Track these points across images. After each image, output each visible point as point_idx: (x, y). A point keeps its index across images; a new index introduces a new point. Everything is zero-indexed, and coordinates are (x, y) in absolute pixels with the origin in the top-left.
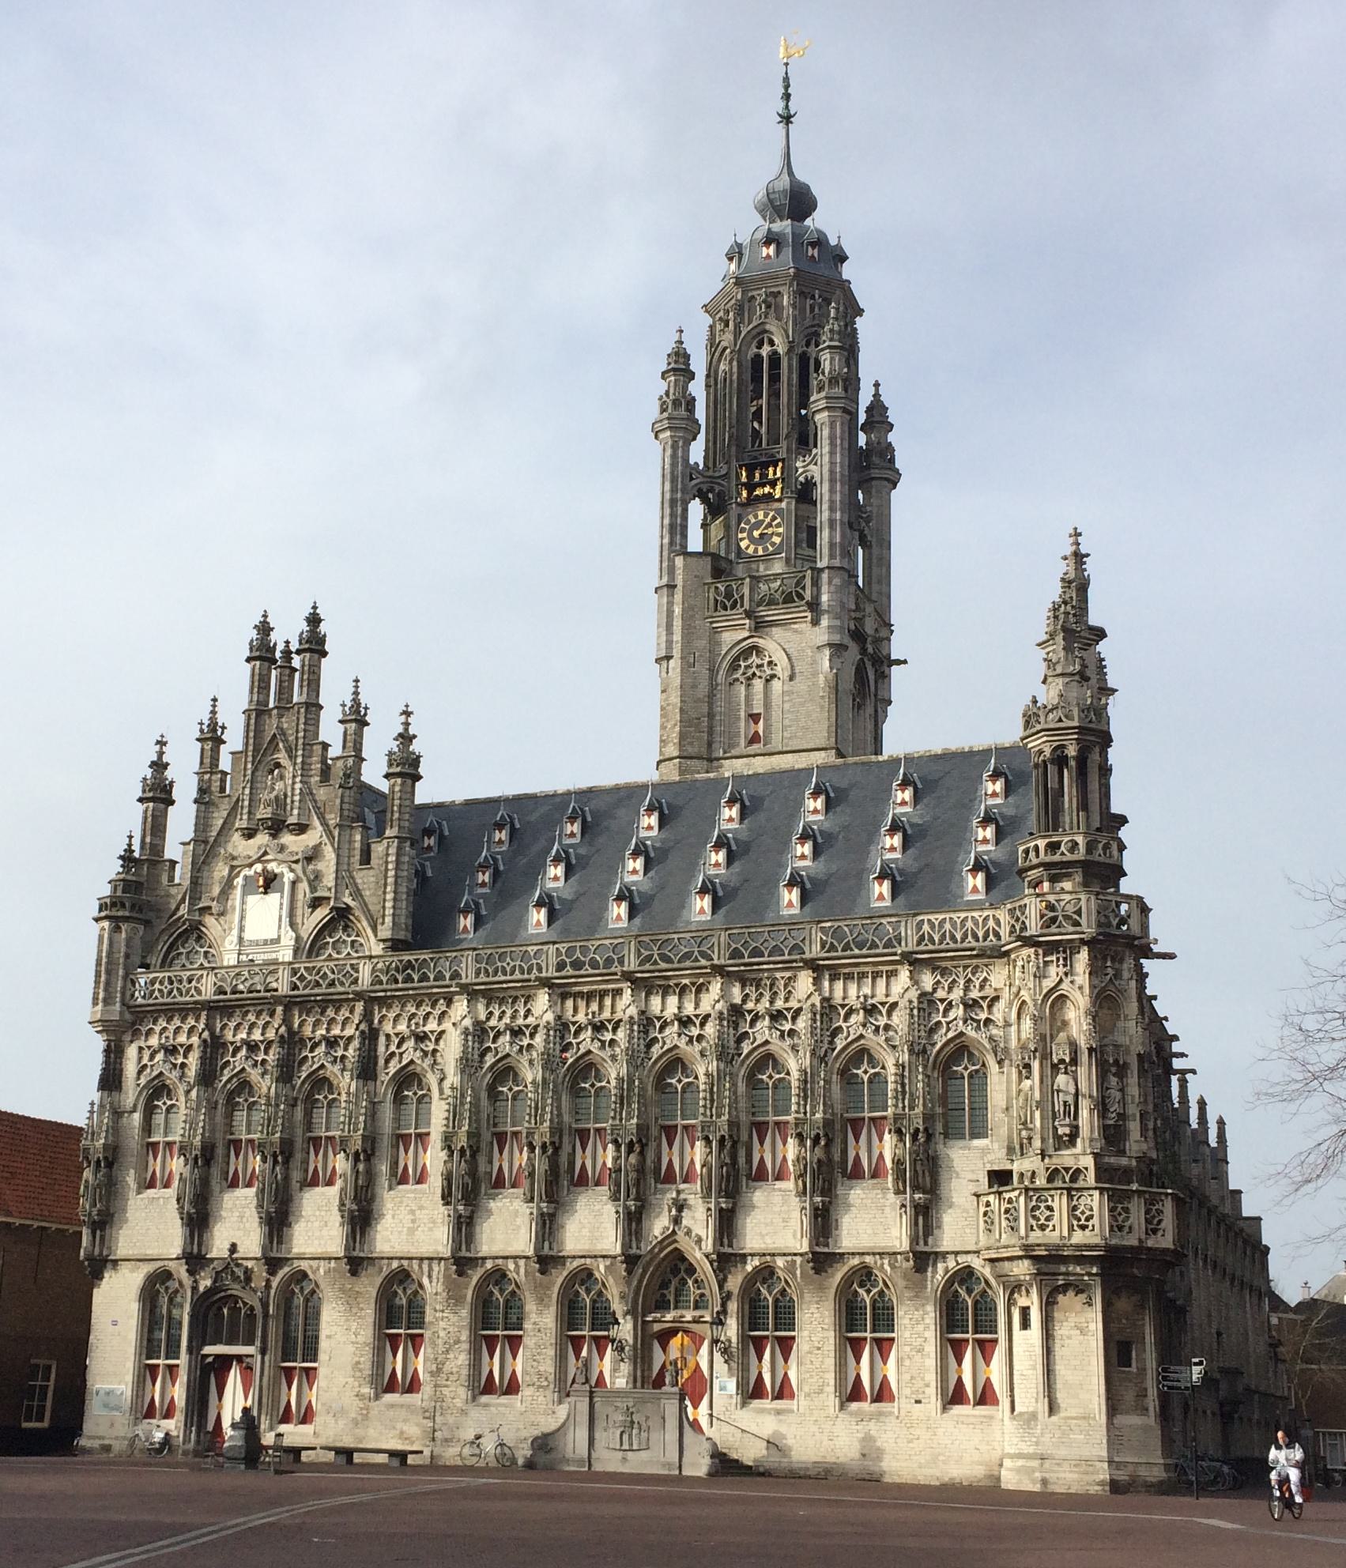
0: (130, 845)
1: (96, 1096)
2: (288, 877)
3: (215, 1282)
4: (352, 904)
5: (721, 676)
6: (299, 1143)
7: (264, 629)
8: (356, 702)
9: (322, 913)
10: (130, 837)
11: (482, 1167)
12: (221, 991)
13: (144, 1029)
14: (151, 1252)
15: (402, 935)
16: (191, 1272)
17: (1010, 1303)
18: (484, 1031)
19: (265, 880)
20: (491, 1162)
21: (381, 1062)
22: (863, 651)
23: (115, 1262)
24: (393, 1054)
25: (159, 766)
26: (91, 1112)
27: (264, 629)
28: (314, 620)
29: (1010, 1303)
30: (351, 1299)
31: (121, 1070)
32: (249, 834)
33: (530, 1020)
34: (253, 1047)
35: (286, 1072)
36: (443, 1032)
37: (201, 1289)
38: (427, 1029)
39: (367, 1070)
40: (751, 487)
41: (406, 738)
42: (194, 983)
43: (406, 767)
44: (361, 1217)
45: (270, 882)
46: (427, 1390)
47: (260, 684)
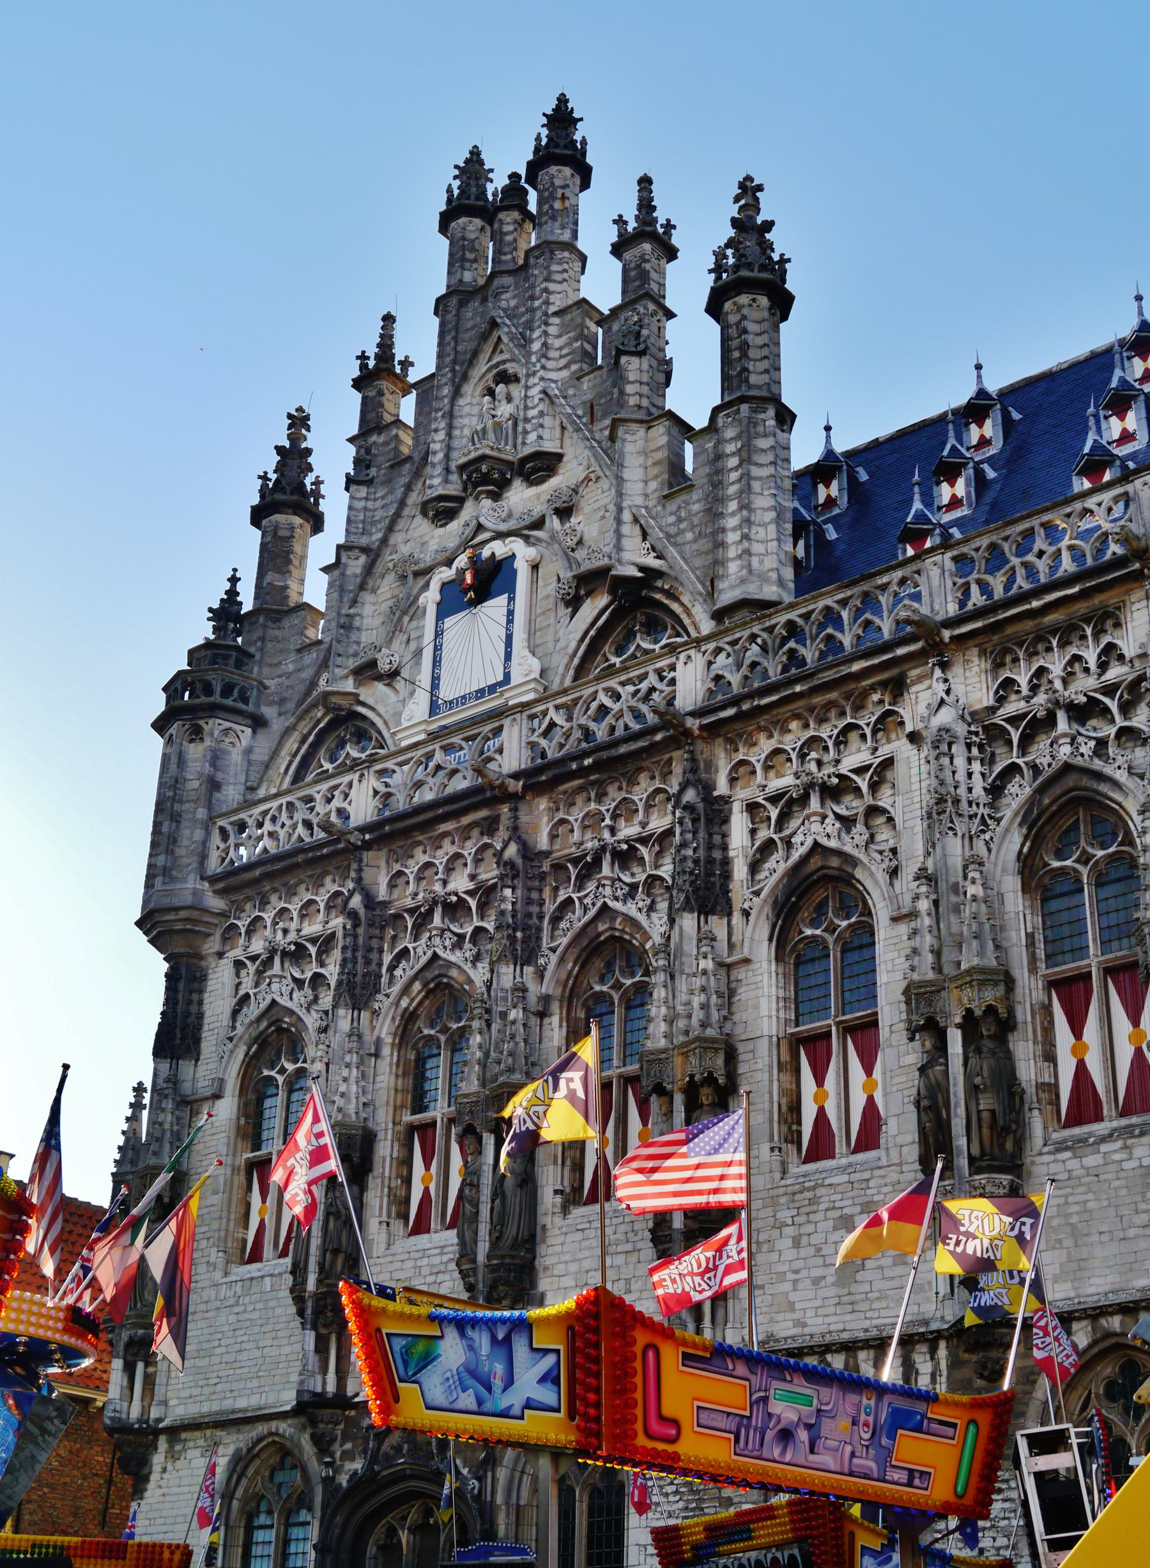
0: (232, 593)
1: (143, 1069)
2: (522, 552)
3: (373, 1460)
4: (656, 563)
9: (595, 606)
10: (234, 580)
11: (1028, 1071)
13: (242, 924)
14: (244, 1403)
15: (770, 592)
16: (323, 1445)
18: (995, 734)
19: (474, 577)
20: (1050, 1057)
21: (740, 871)
23: (174, 1432)
24: (768, 847)
26: (137, 1106)
28: (562, 119)
31: (200, 1016)
32: (442, 511)
33: (1115, 672)
34: (455, 908)
36: (889, 762)
37: (343, 1480)
38: (844, 768)
42: (337, 803)
45: (490, 579)
47: (460, 256)
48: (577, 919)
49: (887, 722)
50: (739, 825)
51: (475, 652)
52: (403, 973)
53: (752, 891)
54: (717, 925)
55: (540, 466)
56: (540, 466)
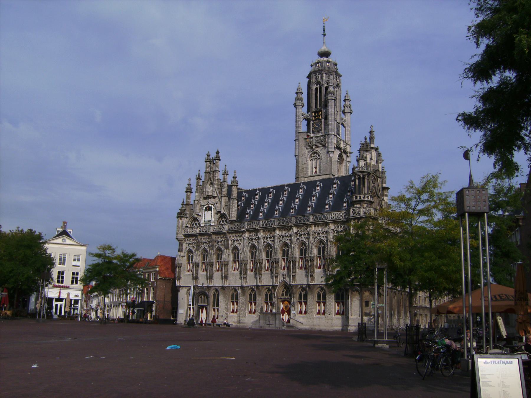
2: (213, 207)
5: (308, 159)
6: (215, 263)
7: (208, 155)
8: (225, 170)
9: (219, 215)
11: (248, 267)
12: (200, 231)
17: (346, 294)
22: (341, 151)
25: (189, 185)
27: (208, 155)
28: (218, 153)
29: (346, 294)
30: (225, 294)
32: (205, 199)
34: (206, 243)
35: (211, 248)
39: (227, 248)
40: (315, 117)
41: (235, 177)
43: (235, 183)
44: (225, 278)
45: (209, 209)
46: (238, 312)
48: (217, 247)
49: (241, 236)
50: (230, 241)
51: (209, 217)
52: (202, 248)
53: (231, 248)
54: (228, 250)
55: (214, 197)
56: (214, 197)
